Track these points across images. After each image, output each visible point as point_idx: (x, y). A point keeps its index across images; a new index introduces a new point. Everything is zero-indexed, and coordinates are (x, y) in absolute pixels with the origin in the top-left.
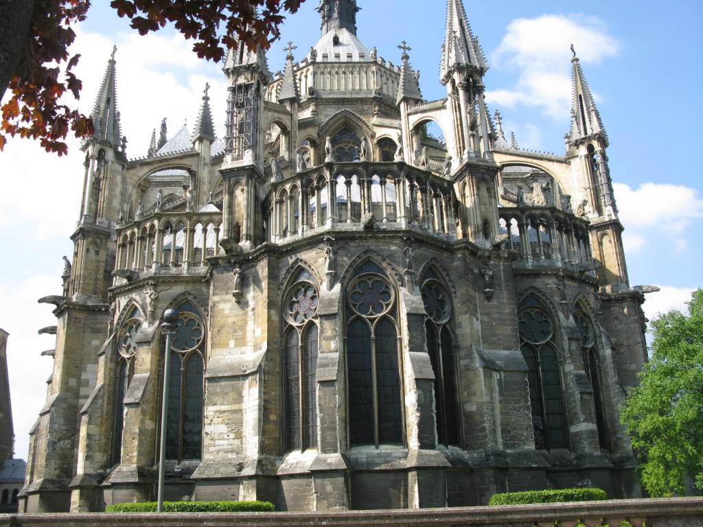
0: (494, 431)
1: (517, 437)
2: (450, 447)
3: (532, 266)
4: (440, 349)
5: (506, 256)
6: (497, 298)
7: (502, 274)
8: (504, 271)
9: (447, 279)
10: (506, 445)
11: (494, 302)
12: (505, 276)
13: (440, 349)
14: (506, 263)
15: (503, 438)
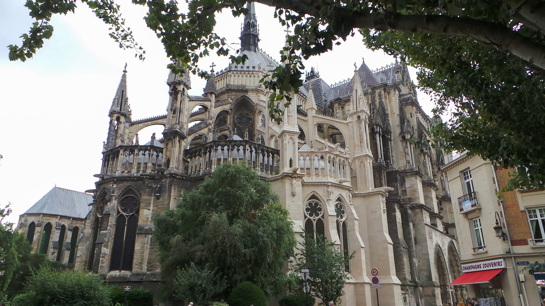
0: (141, 263)
1: (154, 265)
2: (122, 271)
3: (202, 174)
4: (126, 227)
5: (169, 176)
6: (163, 197)
7: (167, 185)
8: (168, 183)
9: (138, 193)
10: (148, 270)
11: (161, 200)
12: (168, 186)
13: (126, 227)
14: (170, 179)
15: (147, 266)
